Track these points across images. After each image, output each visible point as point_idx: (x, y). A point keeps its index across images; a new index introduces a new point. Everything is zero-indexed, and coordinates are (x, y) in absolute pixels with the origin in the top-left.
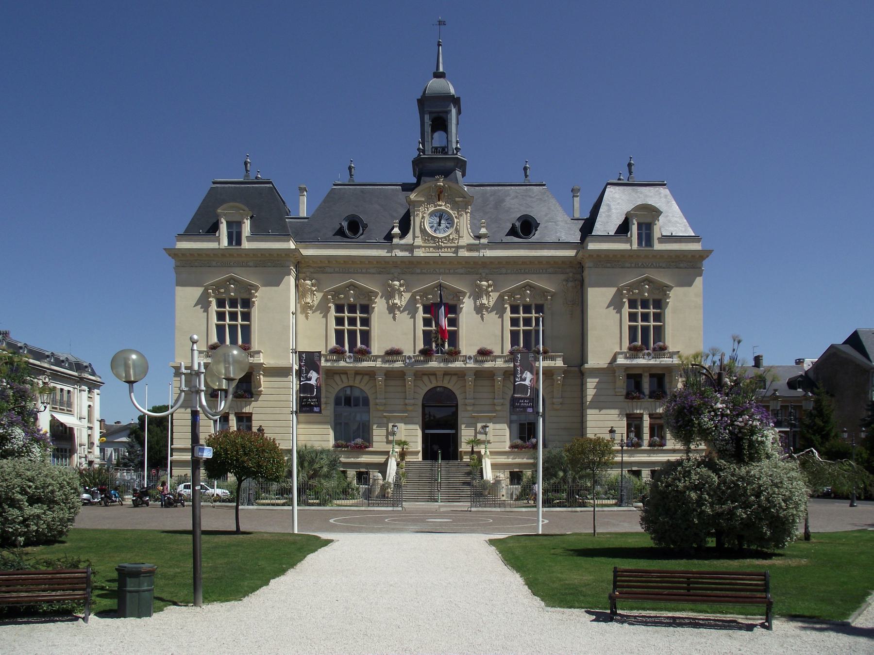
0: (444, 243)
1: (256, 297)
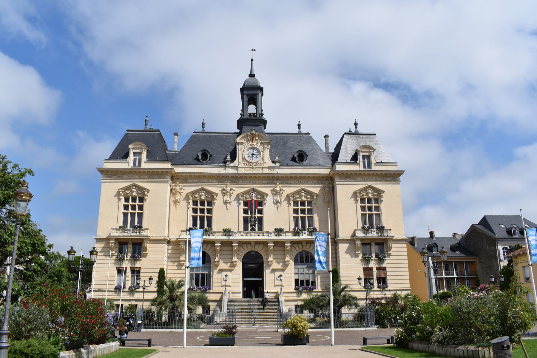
0: (256, 166)
1: (148, 196)
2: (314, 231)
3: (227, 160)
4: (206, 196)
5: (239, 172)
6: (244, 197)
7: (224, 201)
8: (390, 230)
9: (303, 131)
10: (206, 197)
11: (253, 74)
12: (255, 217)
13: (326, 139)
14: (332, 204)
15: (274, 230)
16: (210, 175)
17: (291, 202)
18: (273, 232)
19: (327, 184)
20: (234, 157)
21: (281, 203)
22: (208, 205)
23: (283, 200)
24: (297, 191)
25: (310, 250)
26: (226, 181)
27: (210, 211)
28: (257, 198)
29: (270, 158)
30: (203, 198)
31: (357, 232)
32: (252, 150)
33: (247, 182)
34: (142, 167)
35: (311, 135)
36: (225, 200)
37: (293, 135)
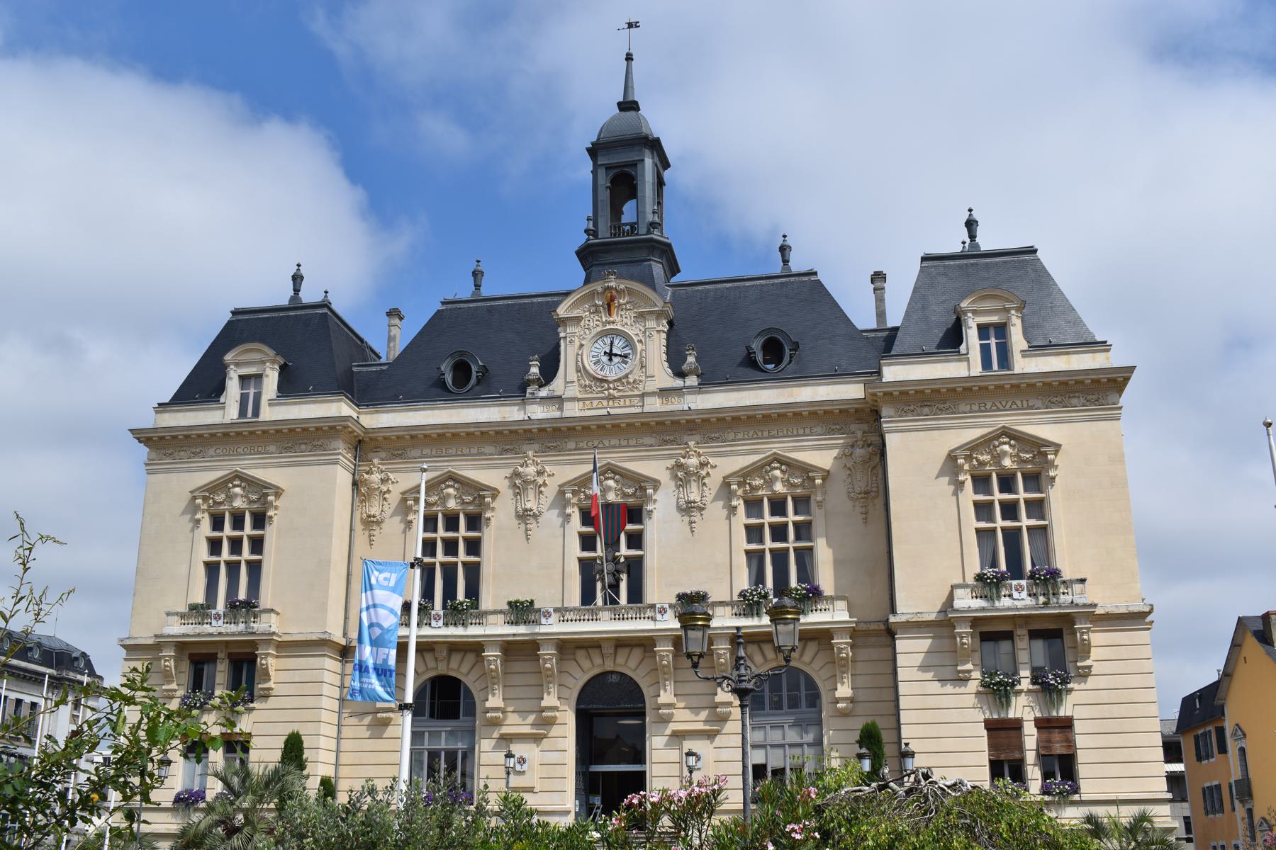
0: (620, 391)
1: (276, 508)
2: (809, 598)
3: (528, 380)
4: (460, 497)
5: (567, 414)
6: (582, 496)
7: (517, 512)
8: (1083, 581)
9: (796, 265)
10: (463, 503)
11: (630, 99)
12: (615, 560)
13: (878, 284)
14: (879, 502)
15: (674, 600)
16: (472, 430)
17: (739, 504)
18: (671, 606)
19: (859, 434)
20: (550, 369)
21: (703, 509)
22: (469, 528)
23: (709, 498)
24: (754, 464)
25: (805, 664)
26: (525, 447)
27: (474, 547)
28: (625, 495)
29: (668, 361)
30: (452, 504)
31: (959, 593)
32: (608, 341)
33: (590, 444)
34: (261, 419)
35: (820, 277)
36: (519, 509)
37: (758, 282)
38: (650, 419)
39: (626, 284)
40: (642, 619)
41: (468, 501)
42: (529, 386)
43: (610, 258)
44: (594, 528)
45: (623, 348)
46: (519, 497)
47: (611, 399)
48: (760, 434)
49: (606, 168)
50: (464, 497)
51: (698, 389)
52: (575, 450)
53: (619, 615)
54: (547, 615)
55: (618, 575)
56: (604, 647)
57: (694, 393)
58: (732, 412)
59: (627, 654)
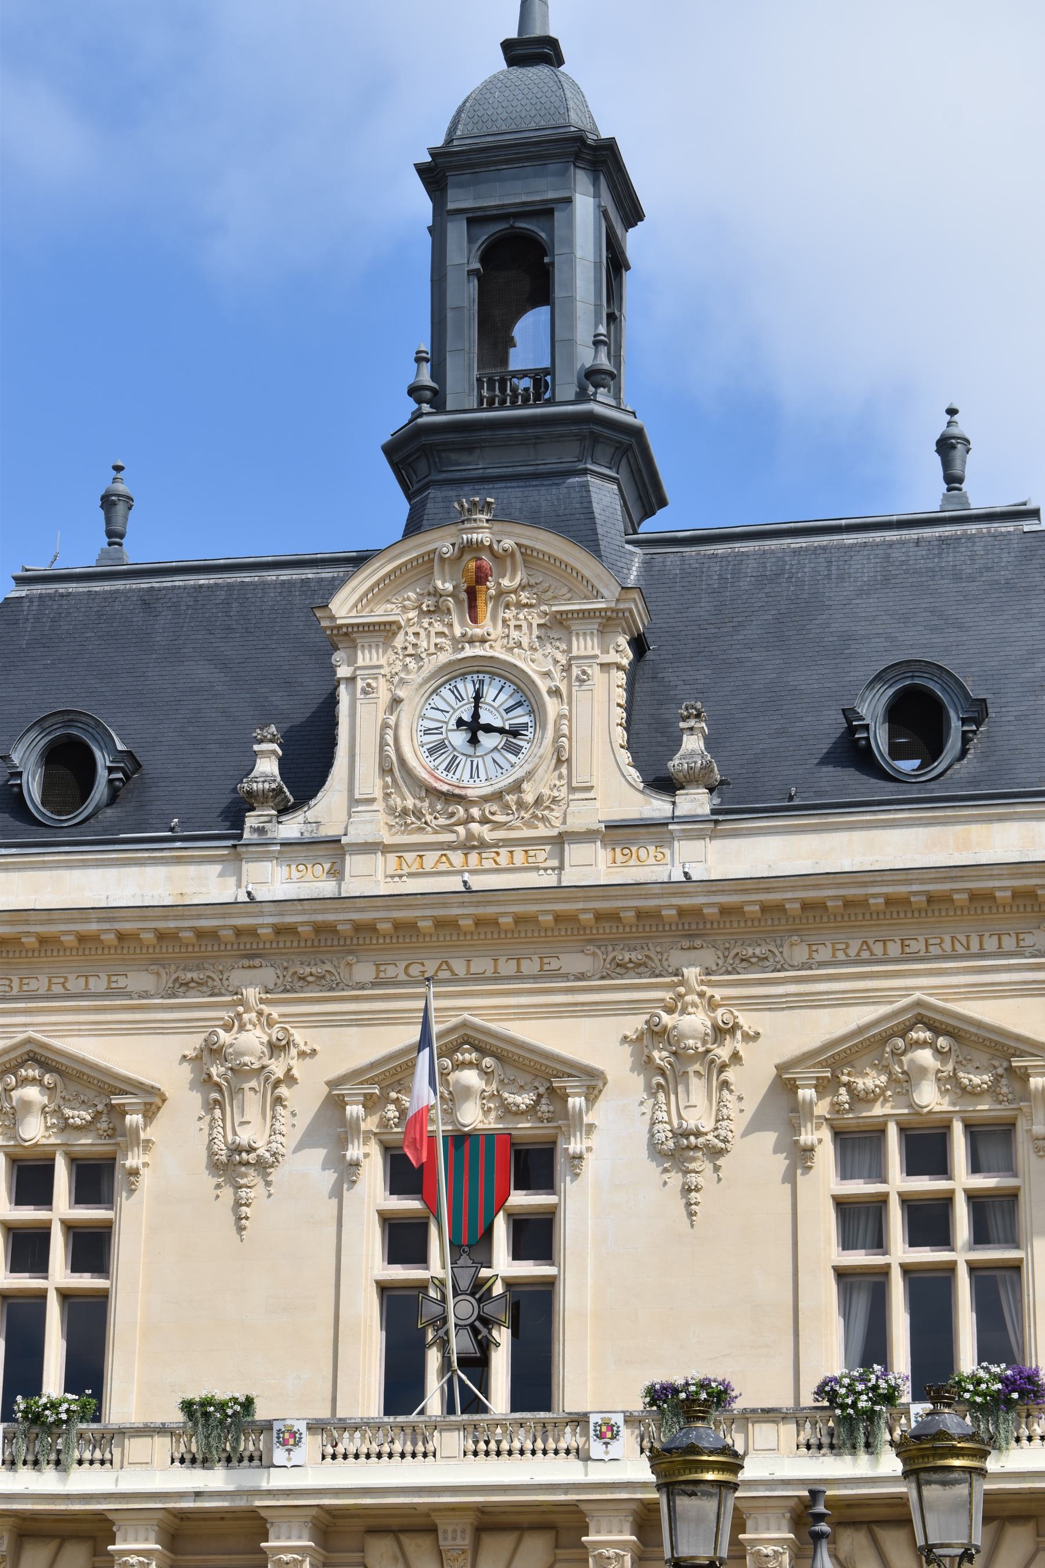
0: (498, 826)
2: (1010, 1404)
3: (250, 793)
4: (58, 1112)
5: (352, 887)
6: (392, 1111)
7: (211, 1154)
10: (66, 1126)
11: (537, 32)
12: (479, 1290)
15: (637, 1404)
16: (94, 927)
18: (630, 1419)
21: (721, 1152)
23: (738, 1122)
24: (861, 1030)
26: (237, 977)
28: (508, 1111)
29: (629, 747)
32: (467, 689)
33: (415, 970)
36: (220, 1145)
37: (877, 536)
38: (580, 905)
39: (519, 535)
40: (551, 1455)
41: (78, 1121)
42: (253, 809)
43: (478, 464)
44: (423, 1199)
45: (508, 710)
46: (218, 1113)
47: (474, 847)
48: (878, 948)
49: (470, 221)
50: (68, 1112)
51: (711, 826)
52: (374, 985)
53: (487, 1443)
54: (290, 1439)
55: (484, 1331)
56: (445, 1532)
57: (700, 836)
58: (805, 887)
59: (505, 1555)
